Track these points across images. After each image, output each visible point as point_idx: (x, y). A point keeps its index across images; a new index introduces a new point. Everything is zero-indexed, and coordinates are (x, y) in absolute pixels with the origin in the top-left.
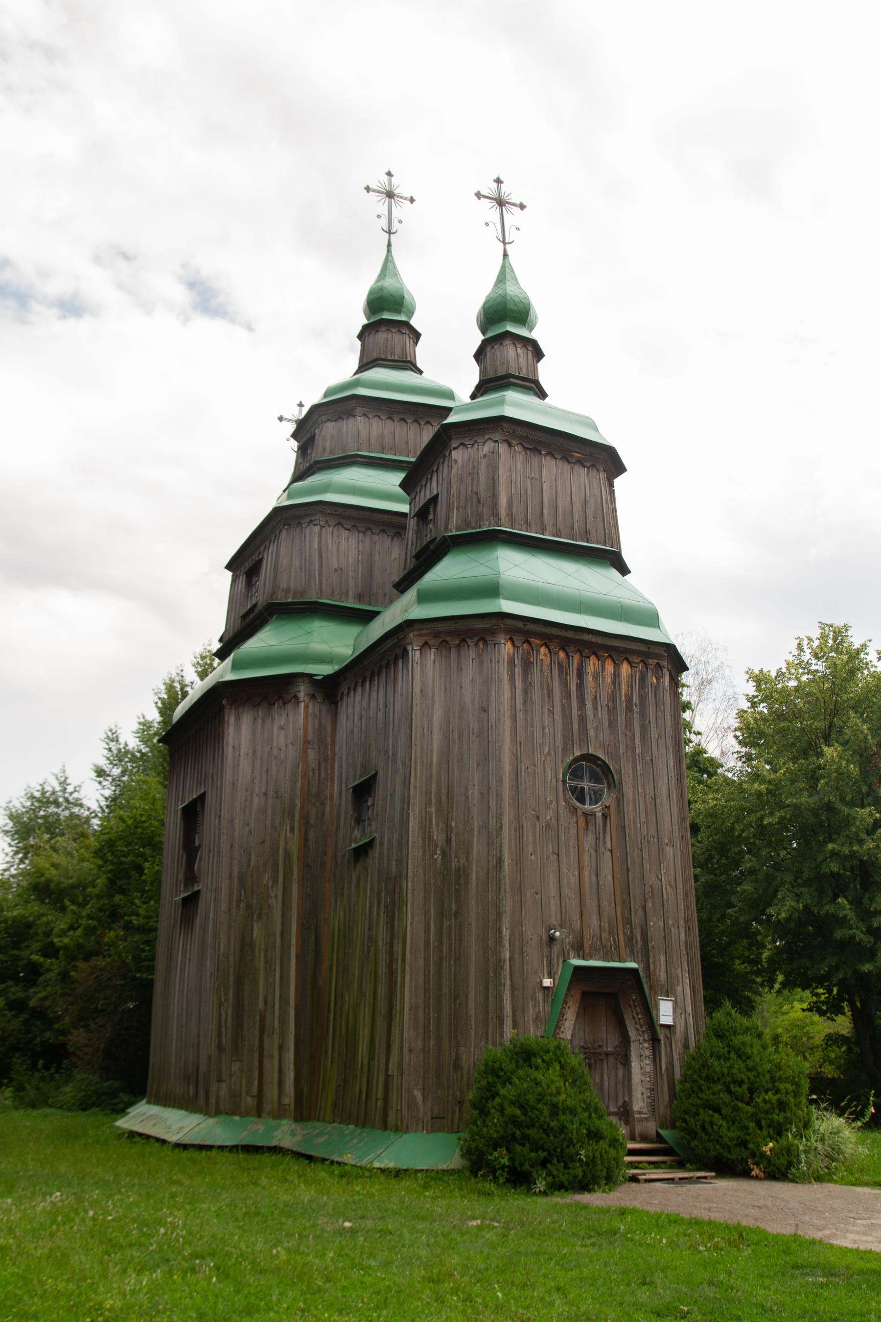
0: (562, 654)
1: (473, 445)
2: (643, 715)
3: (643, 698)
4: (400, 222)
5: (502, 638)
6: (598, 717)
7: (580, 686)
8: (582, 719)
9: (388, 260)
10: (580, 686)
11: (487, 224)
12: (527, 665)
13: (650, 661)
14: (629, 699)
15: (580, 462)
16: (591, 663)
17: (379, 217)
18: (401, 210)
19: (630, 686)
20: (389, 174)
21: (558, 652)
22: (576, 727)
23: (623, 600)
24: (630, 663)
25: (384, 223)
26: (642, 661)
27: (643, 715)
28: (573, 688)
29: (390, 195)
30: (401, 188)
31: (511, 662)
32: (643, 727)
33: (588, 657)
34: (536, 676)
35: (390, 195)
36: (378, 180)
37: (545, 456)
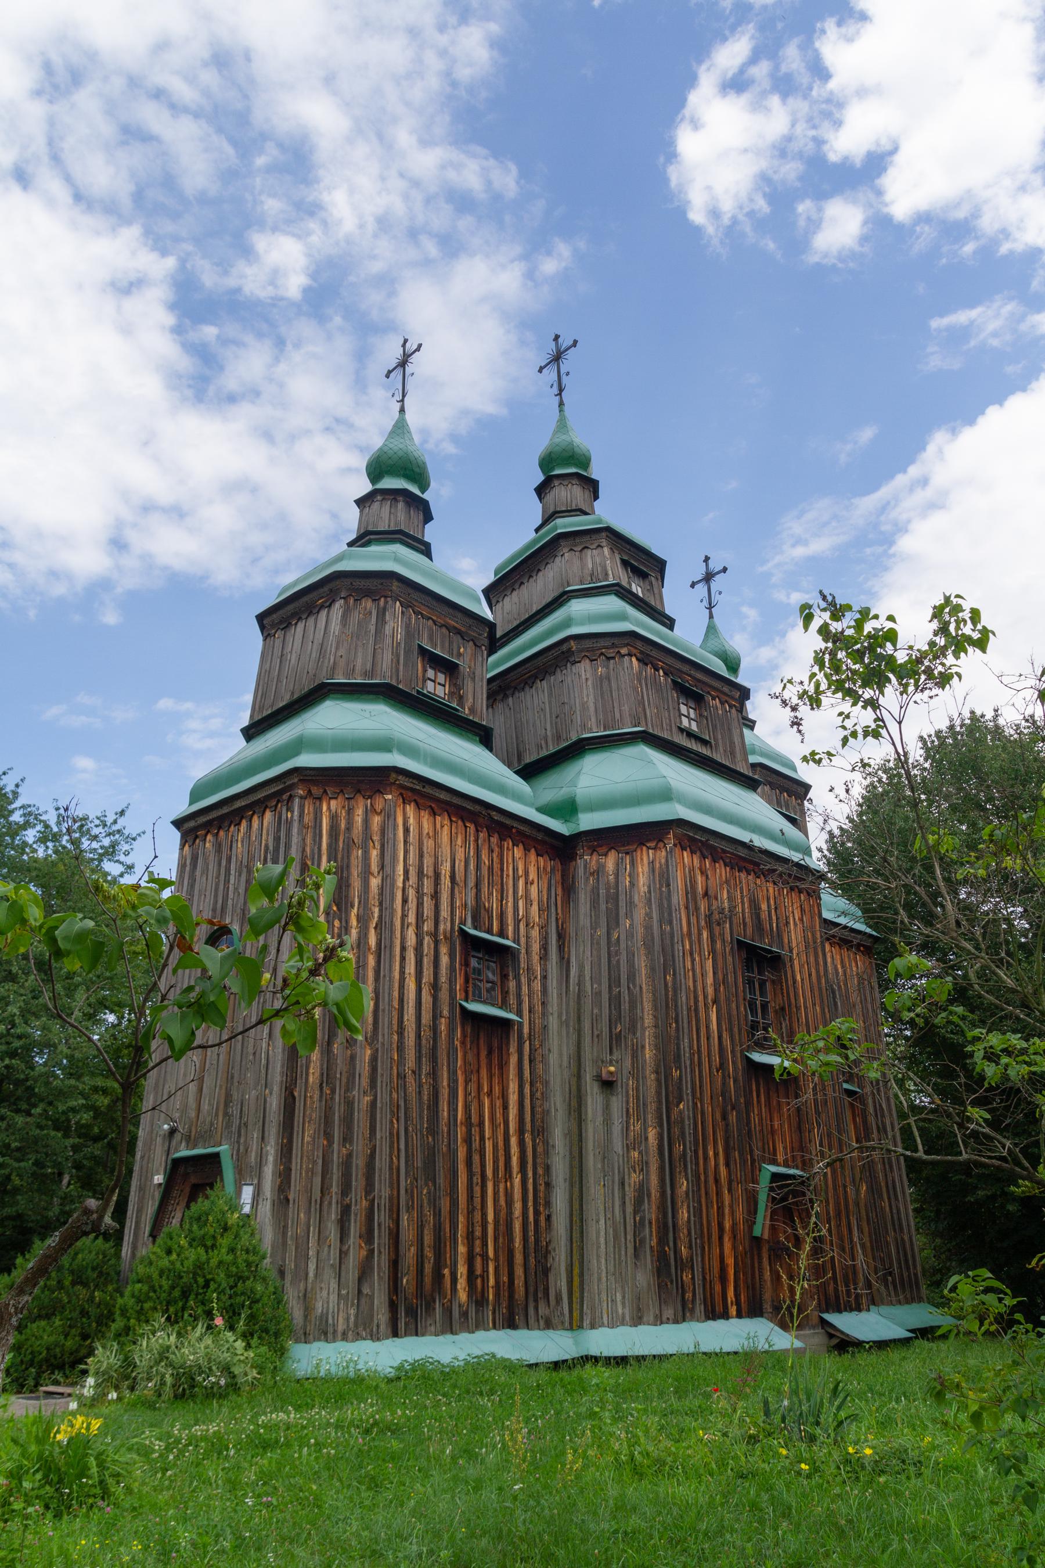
15: (322, 607)
19: (268, 834)
21: (218, 833)
26: (278, 801)
28: (224, 863)
29: (557, 358)
30: (565, 341)
33: (239, 824)
37: (296, 624)
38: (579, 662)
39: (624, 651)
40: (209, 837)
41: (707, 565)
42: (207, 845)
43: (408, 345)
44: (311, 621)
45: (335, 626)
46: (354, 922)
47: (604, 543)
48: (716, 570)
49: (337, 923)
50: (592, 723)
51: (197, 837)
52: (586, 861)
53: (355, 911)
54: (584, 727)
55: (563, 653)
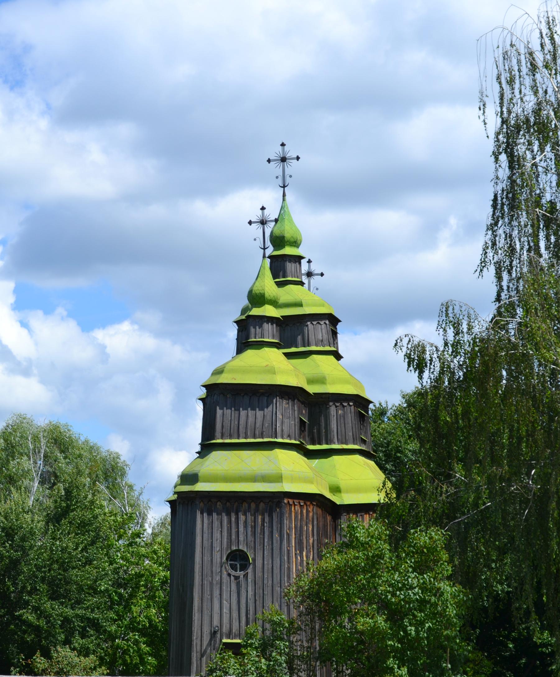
0: (228, 503)
1: (211, 396)
4: (291, 176)
8: (238, 532)
11: (255, 240)
13: (275, 500)
15: (263, 394)
16: (244, 506)
17: (277, 177)
18: (292, 167)
21: (226, 503)
22: (234, 537)
23: (262, 471)
24: (264, 503)
29: (283, 160)
30: (291, 153)
33: (242, 503)
36: (275, 152)
37: (243, 396)
38: (331, 406)
39: (351, 404)
40: (219, 503)
41: (309, 267)
42: (218, 506)
46: (305, 559)
47: (327, 322)
48: (316, 272)
49: (299, 558)
50: (336, 440)
51: (210, 501)
52: (344, 517)
53: (304, 553)
55: (322, 398)
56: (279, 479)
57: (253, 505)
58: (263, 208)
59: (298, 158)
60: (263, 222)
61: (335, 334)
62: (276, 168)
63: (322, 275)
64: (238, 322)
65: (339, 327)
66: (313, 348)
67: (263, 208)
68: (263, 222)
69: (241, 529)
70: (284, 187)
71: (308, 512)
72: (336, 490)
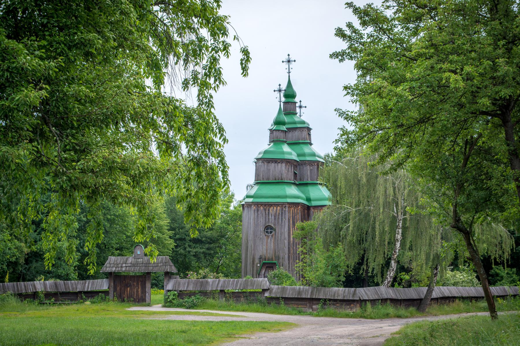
2: (282, 216)
3: (282, 213)
5: (253, 206)
6: (272, 218)
7: (269, 213)
8: (269, 219)
9: (289, 81)
10: (269, 213)
12: (258, 210)
14: (279, 213)
15: (279, 162)
18: (292, 65)
20: (289, 55)
25: (287, 70)
27: (282, 216)
29: (289, 61)
30: (292, 59)
31: (255, 210)
32: (282, 219)
34: (259, 213)
35: (289, 61)
36: (285, 58)
43: (281, 86)
44: (276, 164)
45: (284, 168)
50: (309, 179)
54: (308, 180)
56: (286, 197)
57: (275, 208)
58: (280, 85)
59: (295, 61)
60: (280, 91)
61: (309, 135)
62: (286, 65)
63: (306, 107)
64: (270, 130)
65: (312, 131)
66: (301, 141)
67: (280, 85)
68: (280, 91)
69: (270, 217)
70: (289, 73)
71: (297, 210)
72: (309, 200)
